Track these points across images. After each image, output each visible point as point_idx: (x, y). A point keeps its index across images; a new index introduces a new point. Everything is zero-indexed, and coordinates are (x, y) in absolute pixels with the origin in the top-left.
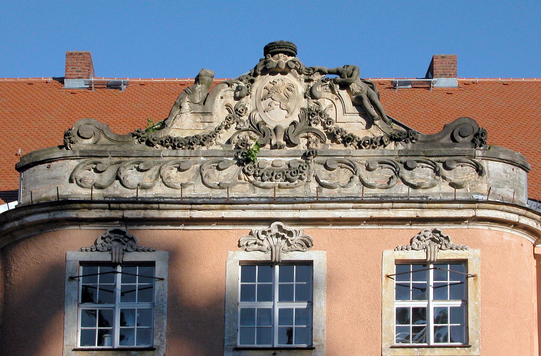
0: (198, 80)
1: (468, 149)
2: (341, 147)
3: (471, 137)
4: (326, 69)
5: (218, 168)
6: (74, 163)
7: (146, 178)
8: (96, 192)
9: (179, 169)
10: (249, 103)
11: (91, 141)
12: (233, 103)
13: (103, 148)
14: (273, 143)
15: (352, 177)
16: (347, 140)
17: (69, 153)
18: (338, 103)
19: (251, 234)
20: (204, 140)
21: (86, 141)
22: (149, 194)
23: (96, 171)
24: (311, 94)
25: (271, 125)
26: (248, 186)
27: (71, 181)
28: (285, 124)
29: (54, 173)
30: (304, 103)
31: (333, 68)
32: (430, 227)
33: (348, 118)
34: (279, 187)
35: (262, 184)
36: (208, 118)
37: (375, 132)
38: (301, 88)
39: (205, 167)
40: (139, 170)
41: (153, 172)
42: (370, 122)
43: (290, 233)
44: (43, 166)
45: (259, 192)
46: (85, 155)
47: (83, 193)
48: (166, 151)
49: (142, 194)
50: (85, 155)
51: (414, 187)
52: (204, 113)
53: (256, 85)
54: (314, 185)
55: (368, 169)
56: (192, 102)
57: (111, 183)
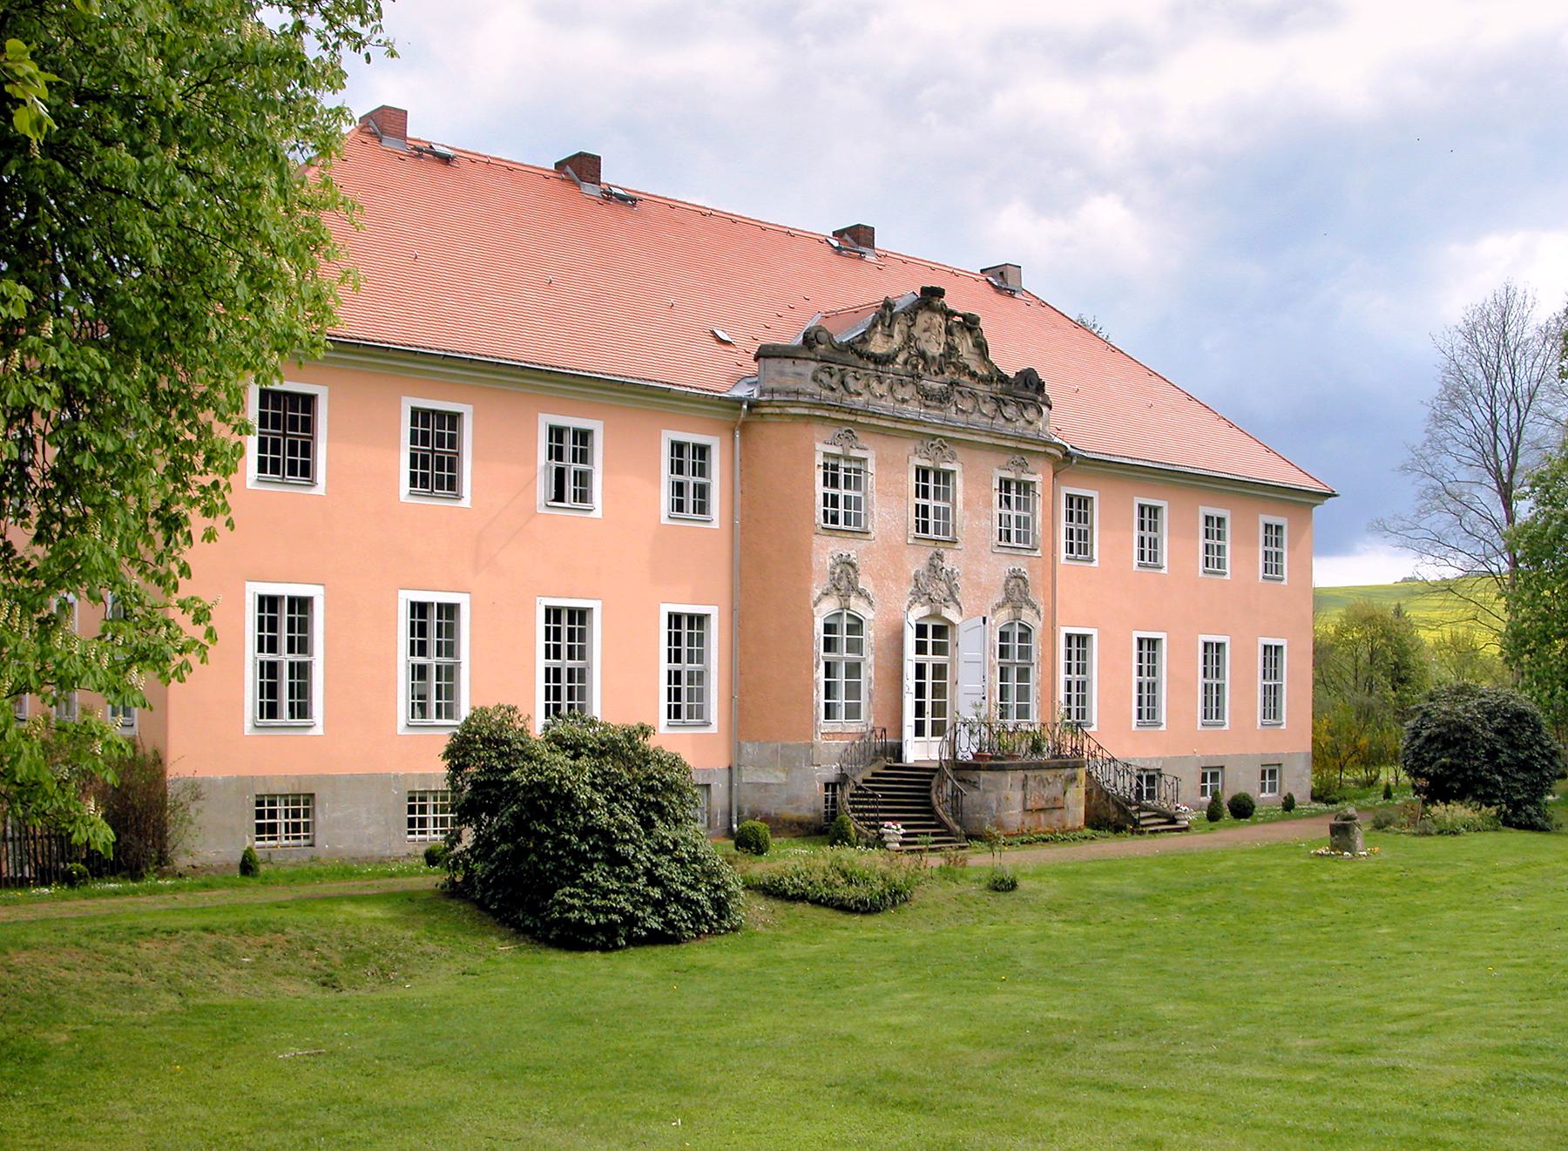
6: (813, 365)
10: (916, 332)
13: (831, 355)
44: (790, 361)
54: (954, 408)
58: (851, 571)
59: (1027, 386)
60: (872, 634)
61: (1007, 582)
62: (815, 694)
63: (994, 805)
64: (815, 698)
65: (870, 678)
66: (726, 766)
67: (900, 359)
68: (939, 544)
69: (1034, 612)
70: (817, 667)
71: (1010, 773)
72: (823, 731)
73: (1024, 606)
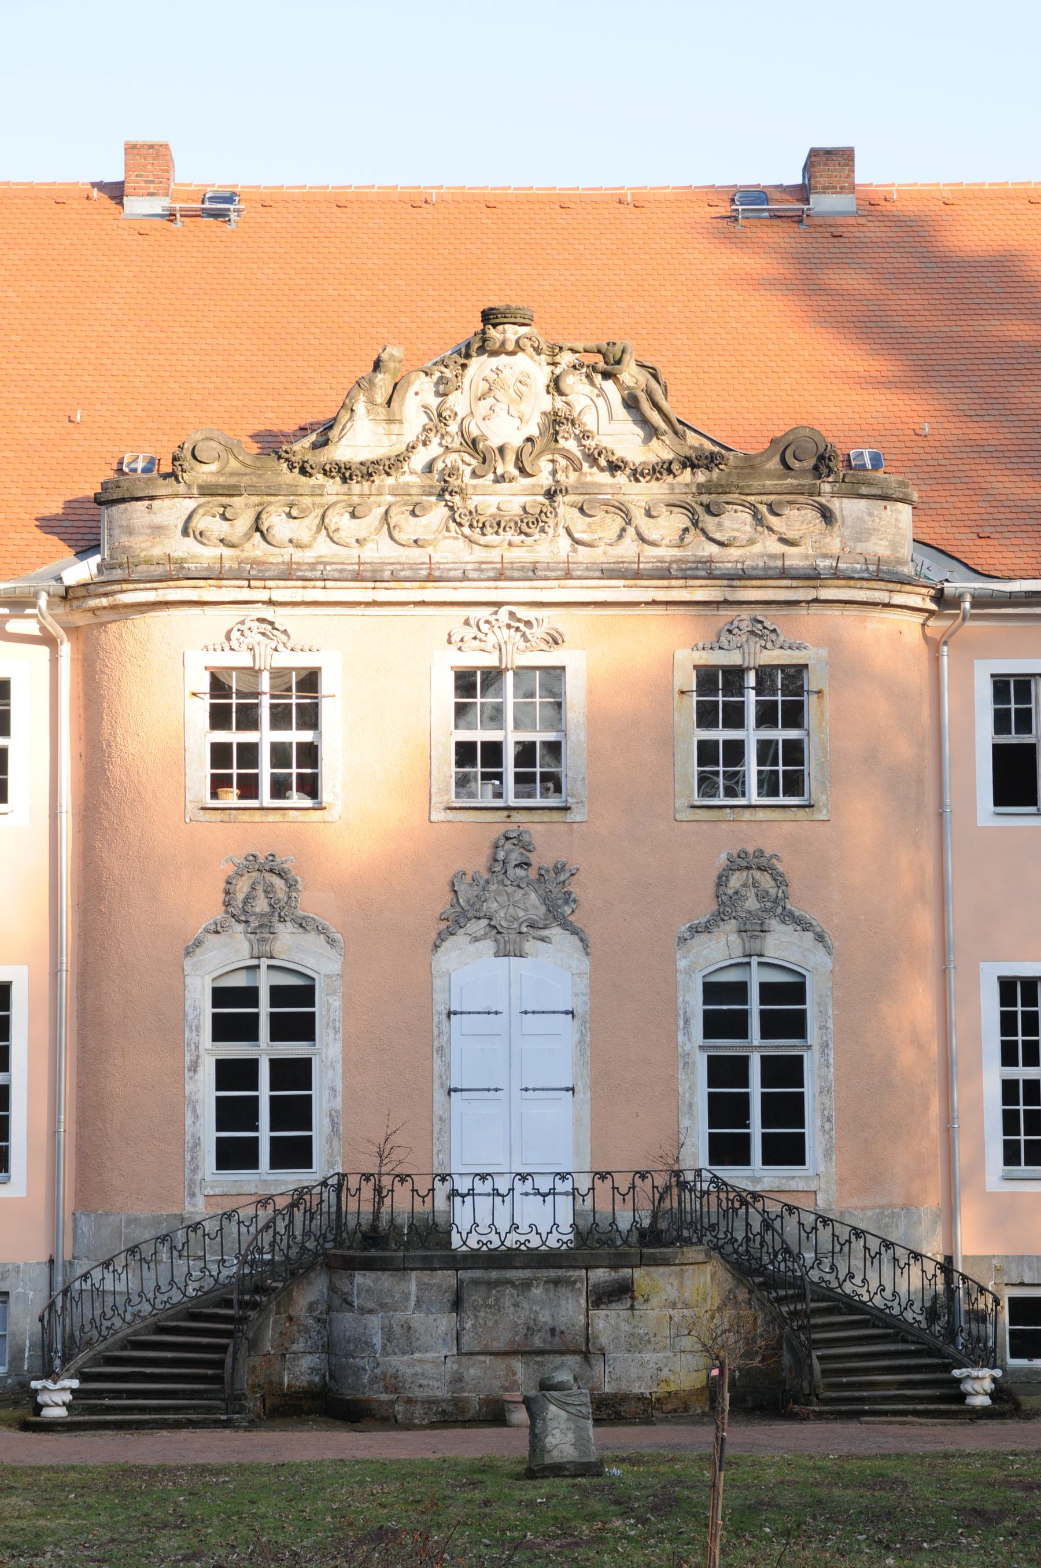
0: (377, 365)
1: (807, 481)
2: (605, 478)
3: (812, 462)
4: (580, 346)
5: (413, 513)
6: (190, 504)
7: (303, 529)
8: (227, 552)
9: (353, 515)
10: (458, 402)
11: (214, 467)
12: (434, 402)
13: (233, 481)
14: (499, 472)
15: (623, 530)
16: (614, 467)
17: (181, 488)
18: (600, 402)
19: (467, 623)
20: (393, 464)
21: (205, 468)
22: (307, 556)
23: (224, 517)
24: (556, 386)
25: (495, 442)
26: (461, 542)
27: (185, 532)
28: (516, 441)
29: (158, 519)
30: (547, 403)
31: (591, 344)
32: (746, 614)
33: (616, 427)
34: (510, 544)
35: (483, 540)
36: (395, 428)
37: (661, 451)
38: (540, 373)
39: (393, 512)
40: (289, 515)
41: (313, 520)
42: (652, 432)
43: (528, 623)
45: (479, 554)
46: (208, 491)
47: (207, 554)
48: (333, 486)
49: (298, 556)
50: (208, 491)
51: (721, 544)
52: (390, 421)
53: (470, 372)
54: (565, 542)
55: (649, 514)
56: (371, 402)
57: (248, 537)
58: (278, 883)
59: (788, 467)
60: (336, 1002)
61: (722, 881)
62: (188, 1121)
63: (378, 1340)
64: (189, 1130)
65: (333, 1089)
66: (45, 1259)
67: (419, 459)
68: (517, 817)
69: (810, 935)
70: (194, 1067)
71: (414, 1274)
72: (209, 1191)
73: (774, 924)
